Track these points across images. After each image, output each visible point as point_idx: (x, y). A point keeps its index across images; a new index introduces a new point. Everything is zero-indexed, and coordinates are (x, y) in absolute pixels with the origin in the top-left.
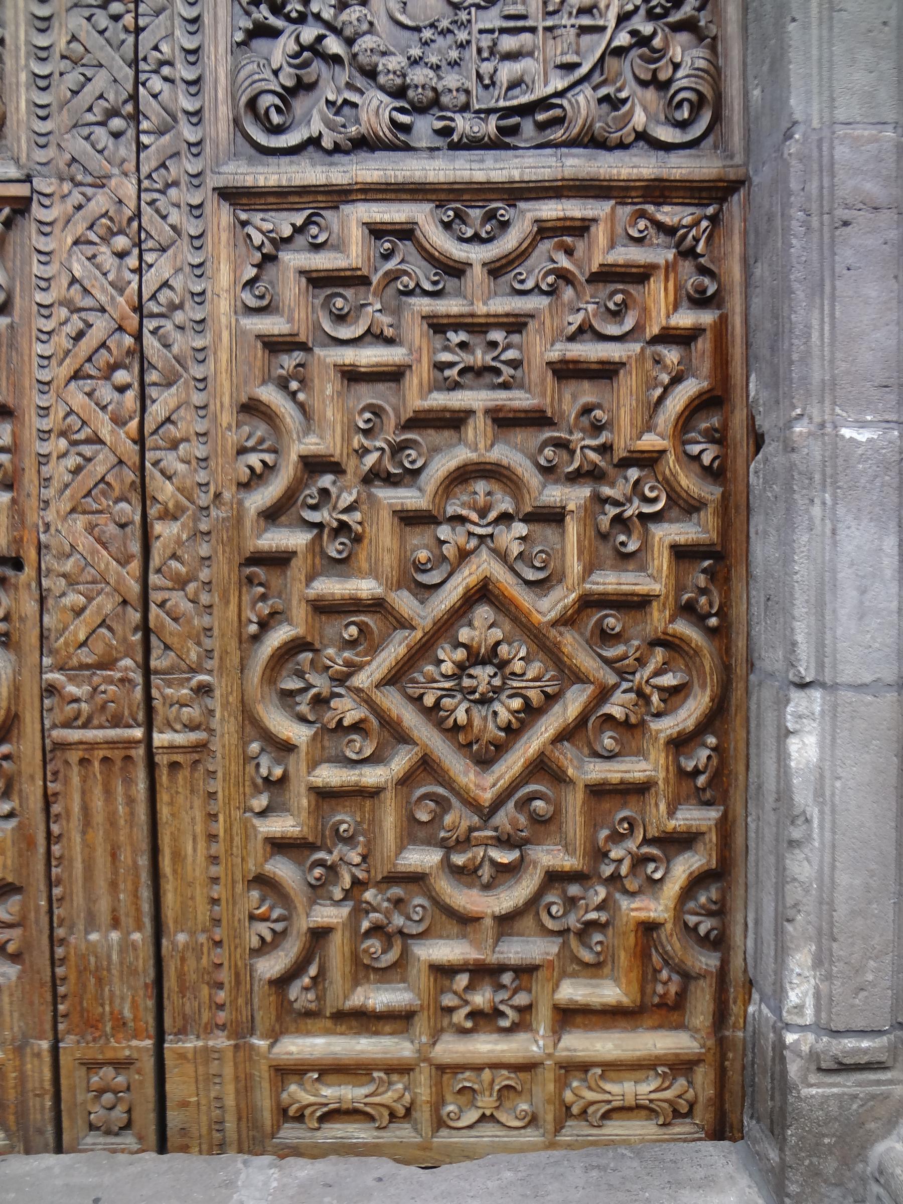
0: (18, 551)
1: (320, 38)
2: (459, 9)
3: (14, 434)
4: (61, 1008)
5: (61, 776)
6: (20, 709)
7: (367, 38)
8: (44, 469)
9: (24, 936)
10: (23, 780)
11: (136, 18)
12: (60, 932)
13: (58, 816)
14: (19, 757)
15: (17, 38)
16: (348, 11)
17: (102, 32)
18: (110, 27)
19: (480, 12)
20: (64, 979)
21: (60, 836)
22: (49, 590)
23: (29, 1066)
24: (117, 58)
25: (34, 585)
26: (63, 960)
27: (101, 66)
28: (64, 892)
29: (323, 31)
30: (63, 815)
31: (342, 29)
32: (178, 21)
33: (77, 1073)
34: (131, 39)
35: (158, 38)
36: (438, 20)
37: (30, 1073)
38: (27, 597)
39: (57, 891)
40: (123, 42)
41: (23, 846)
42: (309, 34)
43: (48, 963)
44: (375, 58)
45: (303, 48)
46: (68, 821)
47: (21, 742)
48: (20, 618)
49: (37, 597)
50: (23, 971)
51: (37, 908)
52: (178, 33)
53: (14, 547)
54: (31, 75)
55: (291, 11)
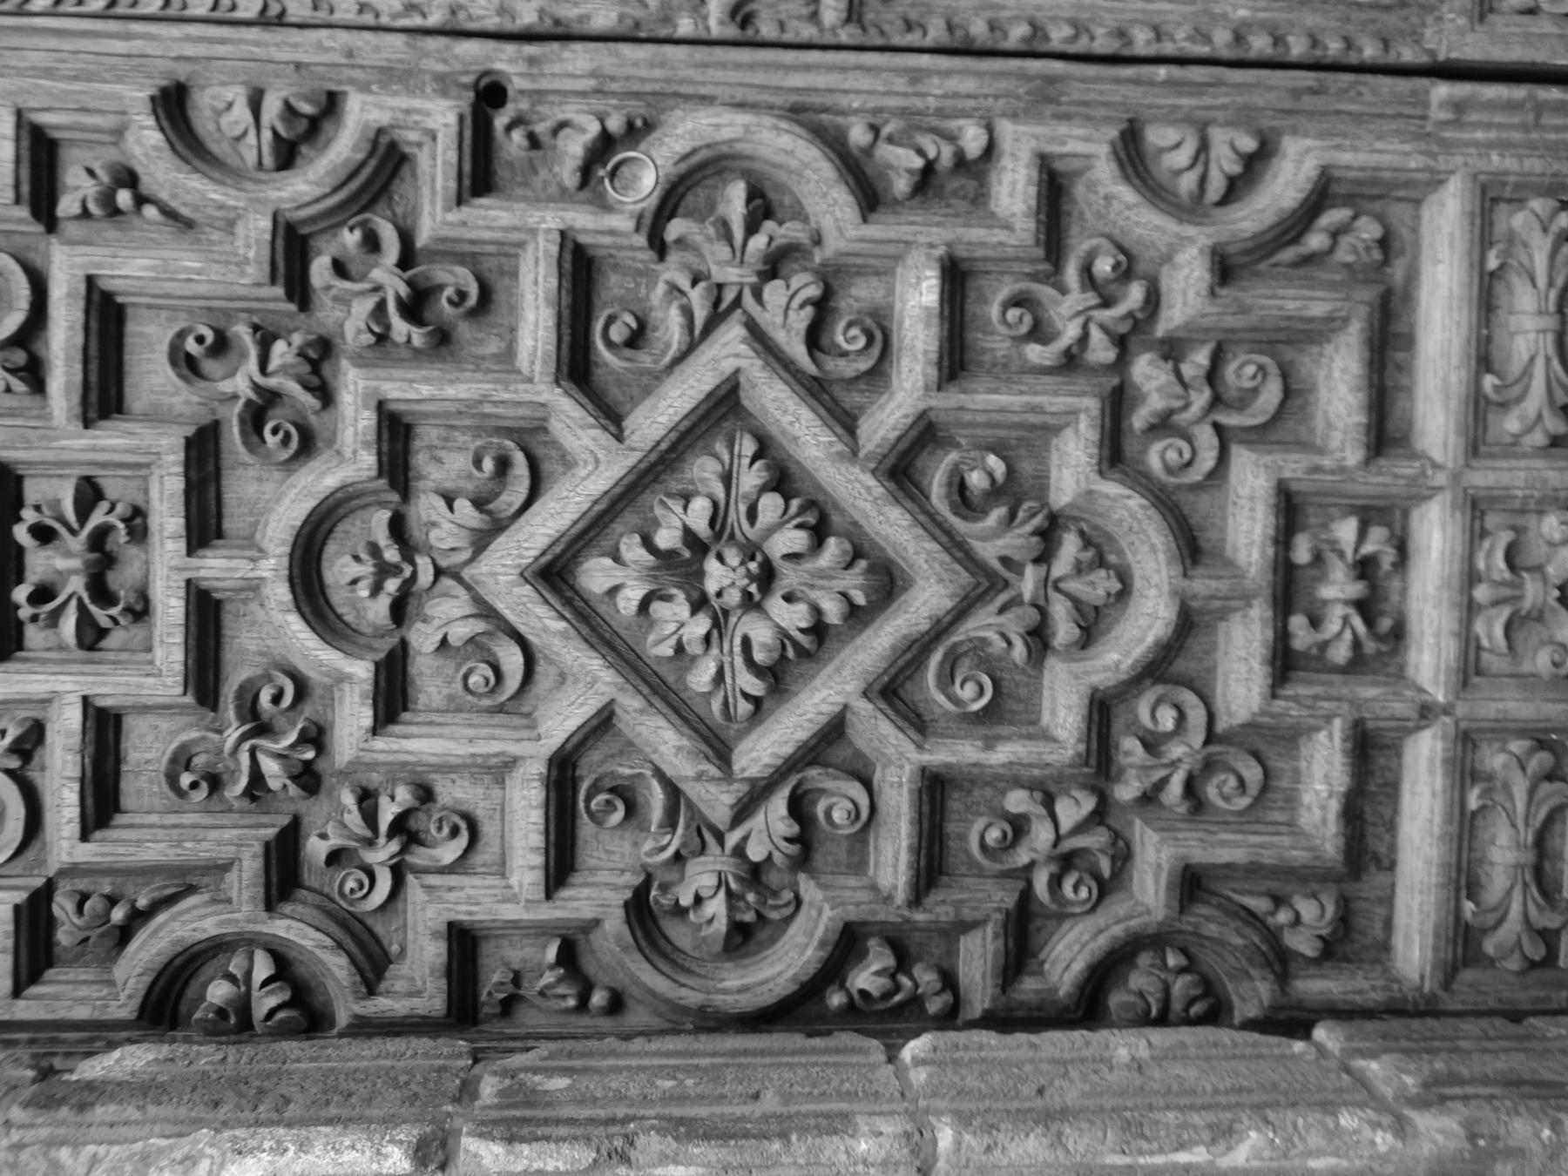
0: (464, 86)
3: (224, 84)
4: (1370, 51)
5: (913, 15)
6: (778, 100)
8: (291, 17)
9: (1228, 124)
10: (918, 103)
12: (1222, 39)
13: (993, 26)
14: (877, 111)
20: (1315, 43)
21: (1032, 24)
22: (542, 12)
23: (1479, 135)
25: (531, 49)
26: (1278, 41)
28: (1144, 23)
30: (989, 14)
33: (1501, 29)
37: (1492, 135)
38: (556, 68)
39: (1142, 42)
41: (1049, 109)
43: (1279, 74)
46: (1003, 7)
47: (843, 101)
48: (599, 92)
49: (555, 46)
50: (1295, 131)
51: (1170, 83)
53: (455, 91)
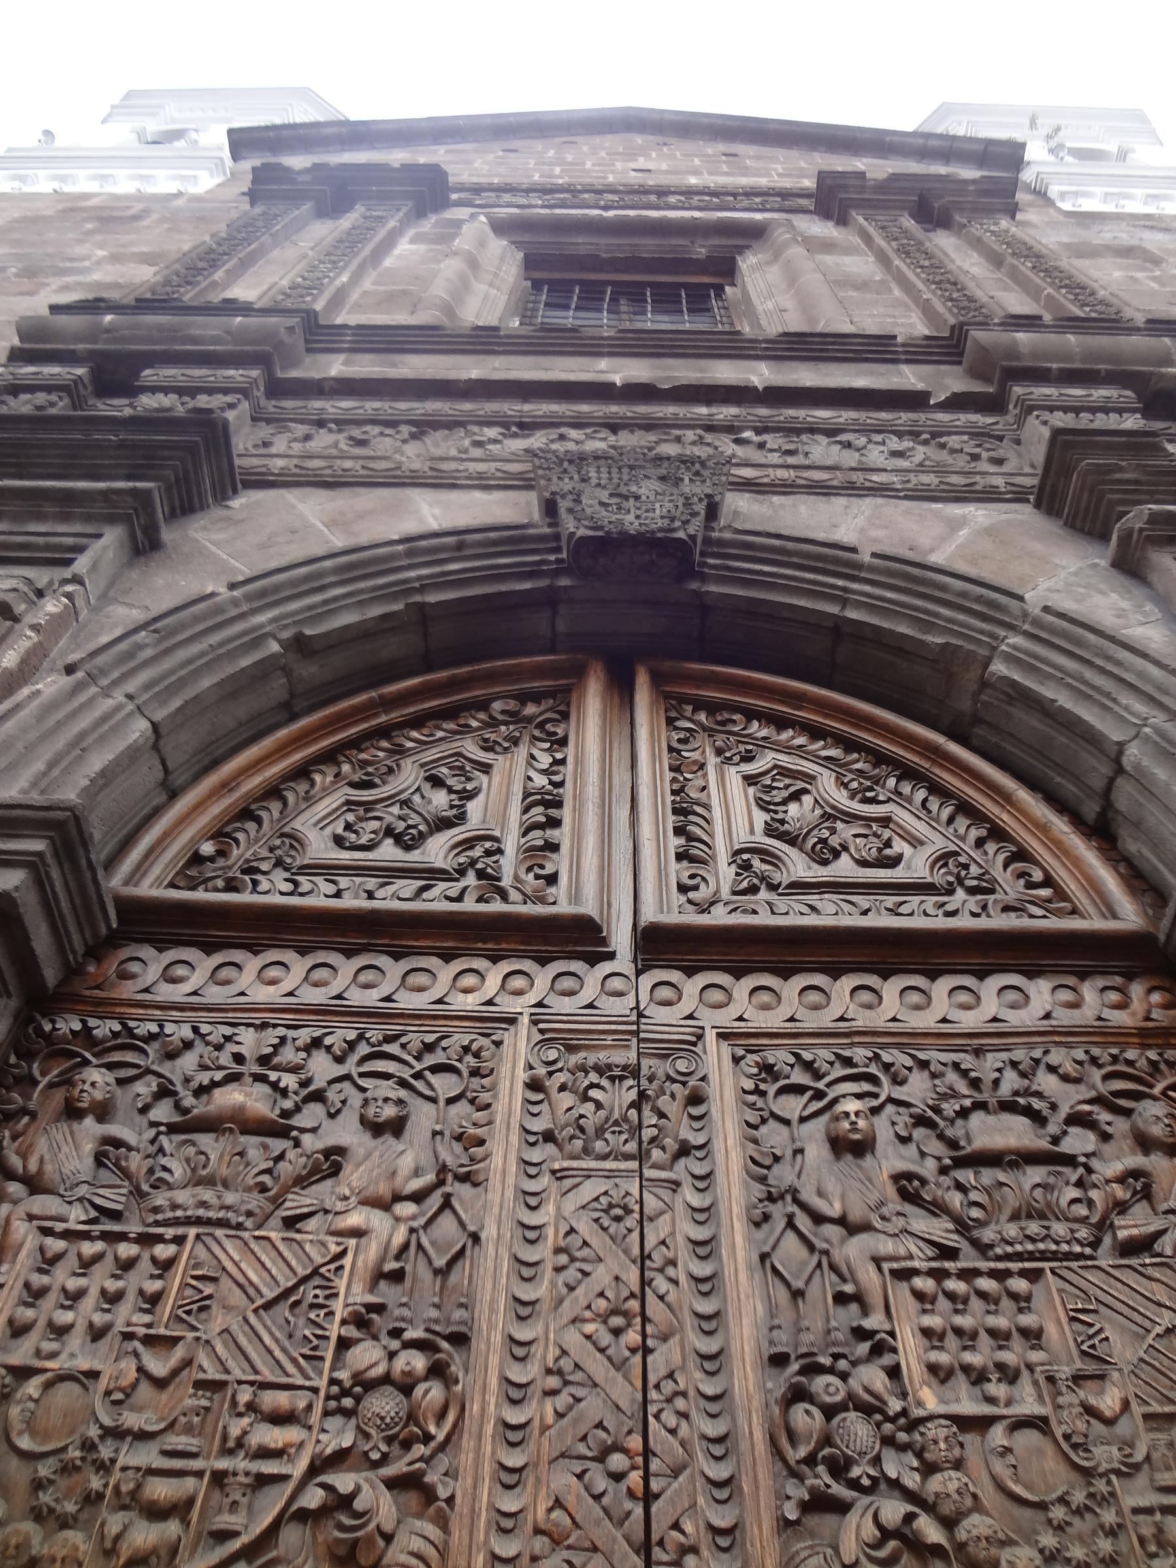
1: (909, 1518)
2: (1093, 1476)
7: (975, 1518)
11: (646, 1478)
15: (474, 1498)
16: (938, 1477)
17: (597, 1497)
18: (610, 1489)
19: (1127, 1483)
24: (618, 1535)
27: (595, 1549)
29: (911, 1508)
31: (935, 1504)
32: (700, 1483)
34: (639, 1511)
35: (679, 1511)
36: (1068, 1493)
40: (629, 1514)
42: (893, 1510)
44: (994, 1551)
45: (886, 1534)
52: (701, 1501)
54: (489, 1556)
55: (860, 1477)
